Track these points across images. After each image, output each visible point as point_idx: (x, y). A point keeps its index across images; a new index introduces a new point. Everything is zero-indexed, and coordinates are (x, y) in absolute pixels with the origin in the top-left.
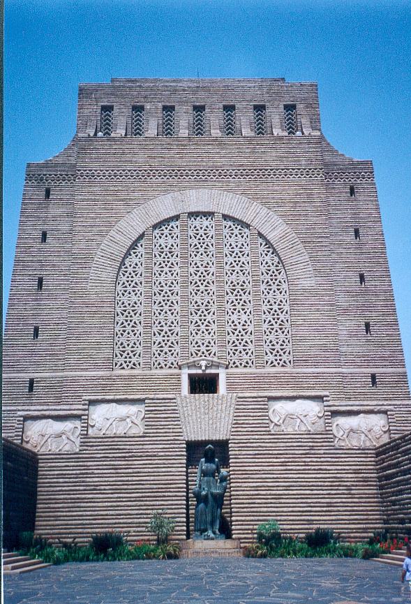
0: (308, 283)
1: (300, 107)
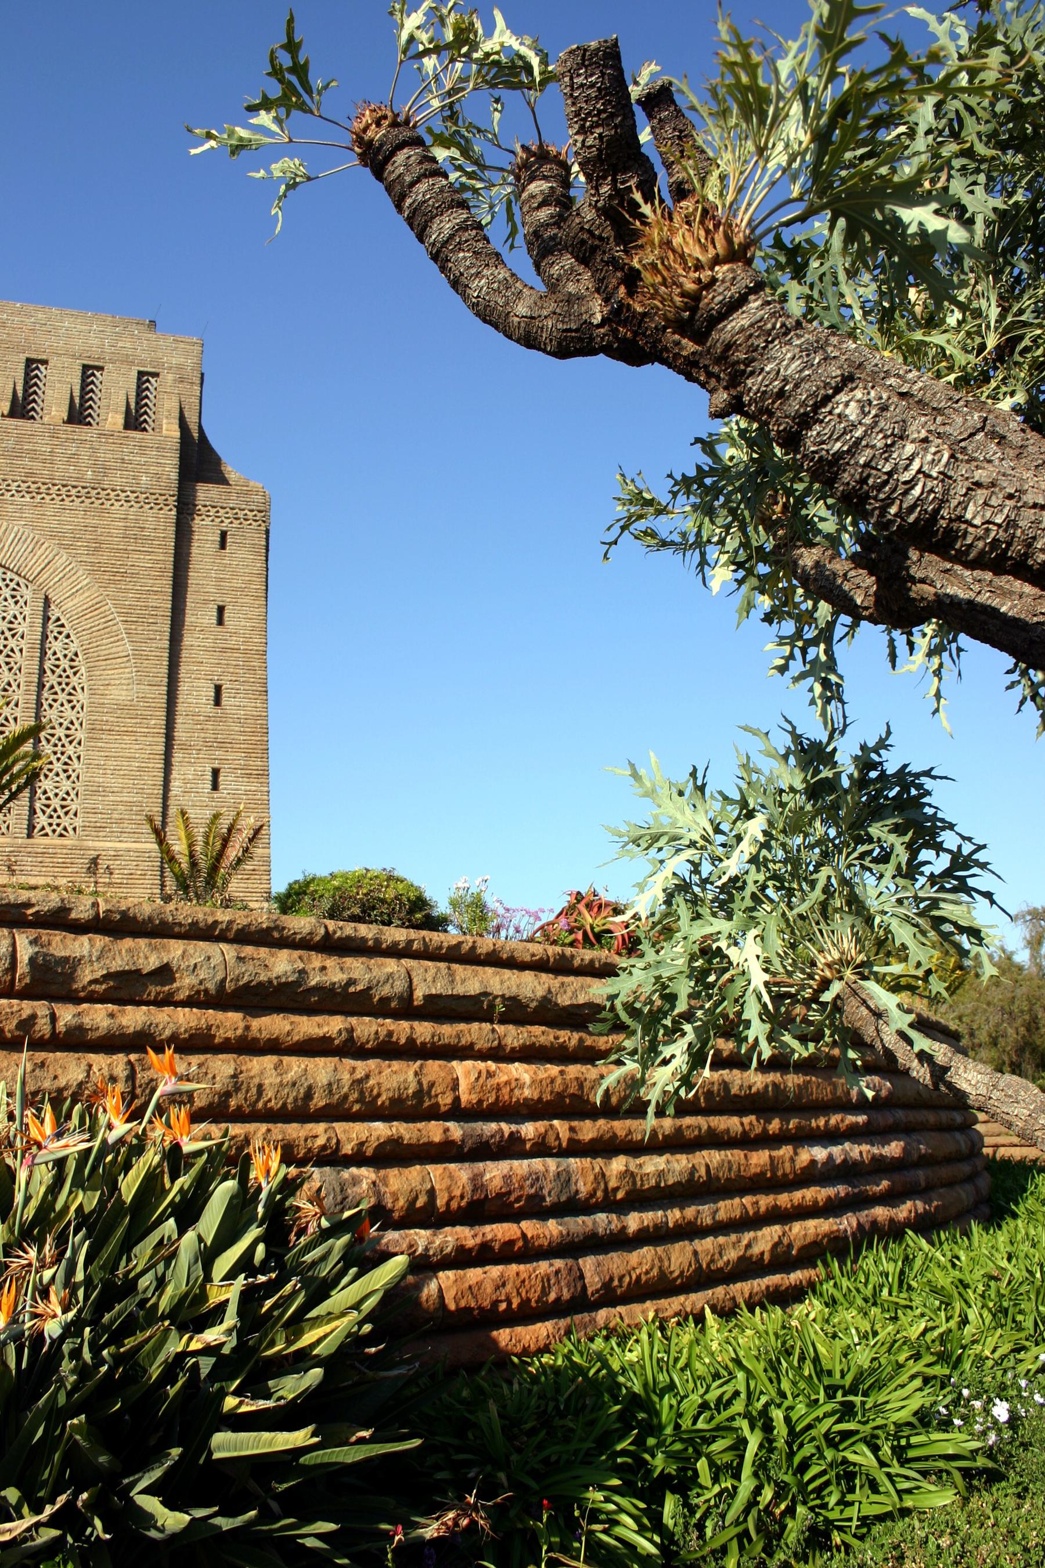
0: (119, 694)
1: (168, 378)
